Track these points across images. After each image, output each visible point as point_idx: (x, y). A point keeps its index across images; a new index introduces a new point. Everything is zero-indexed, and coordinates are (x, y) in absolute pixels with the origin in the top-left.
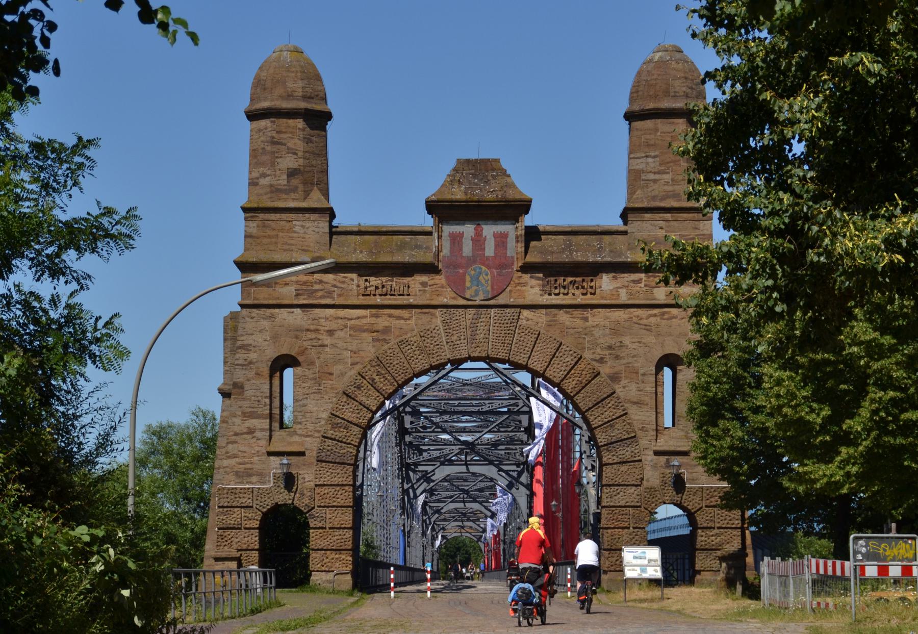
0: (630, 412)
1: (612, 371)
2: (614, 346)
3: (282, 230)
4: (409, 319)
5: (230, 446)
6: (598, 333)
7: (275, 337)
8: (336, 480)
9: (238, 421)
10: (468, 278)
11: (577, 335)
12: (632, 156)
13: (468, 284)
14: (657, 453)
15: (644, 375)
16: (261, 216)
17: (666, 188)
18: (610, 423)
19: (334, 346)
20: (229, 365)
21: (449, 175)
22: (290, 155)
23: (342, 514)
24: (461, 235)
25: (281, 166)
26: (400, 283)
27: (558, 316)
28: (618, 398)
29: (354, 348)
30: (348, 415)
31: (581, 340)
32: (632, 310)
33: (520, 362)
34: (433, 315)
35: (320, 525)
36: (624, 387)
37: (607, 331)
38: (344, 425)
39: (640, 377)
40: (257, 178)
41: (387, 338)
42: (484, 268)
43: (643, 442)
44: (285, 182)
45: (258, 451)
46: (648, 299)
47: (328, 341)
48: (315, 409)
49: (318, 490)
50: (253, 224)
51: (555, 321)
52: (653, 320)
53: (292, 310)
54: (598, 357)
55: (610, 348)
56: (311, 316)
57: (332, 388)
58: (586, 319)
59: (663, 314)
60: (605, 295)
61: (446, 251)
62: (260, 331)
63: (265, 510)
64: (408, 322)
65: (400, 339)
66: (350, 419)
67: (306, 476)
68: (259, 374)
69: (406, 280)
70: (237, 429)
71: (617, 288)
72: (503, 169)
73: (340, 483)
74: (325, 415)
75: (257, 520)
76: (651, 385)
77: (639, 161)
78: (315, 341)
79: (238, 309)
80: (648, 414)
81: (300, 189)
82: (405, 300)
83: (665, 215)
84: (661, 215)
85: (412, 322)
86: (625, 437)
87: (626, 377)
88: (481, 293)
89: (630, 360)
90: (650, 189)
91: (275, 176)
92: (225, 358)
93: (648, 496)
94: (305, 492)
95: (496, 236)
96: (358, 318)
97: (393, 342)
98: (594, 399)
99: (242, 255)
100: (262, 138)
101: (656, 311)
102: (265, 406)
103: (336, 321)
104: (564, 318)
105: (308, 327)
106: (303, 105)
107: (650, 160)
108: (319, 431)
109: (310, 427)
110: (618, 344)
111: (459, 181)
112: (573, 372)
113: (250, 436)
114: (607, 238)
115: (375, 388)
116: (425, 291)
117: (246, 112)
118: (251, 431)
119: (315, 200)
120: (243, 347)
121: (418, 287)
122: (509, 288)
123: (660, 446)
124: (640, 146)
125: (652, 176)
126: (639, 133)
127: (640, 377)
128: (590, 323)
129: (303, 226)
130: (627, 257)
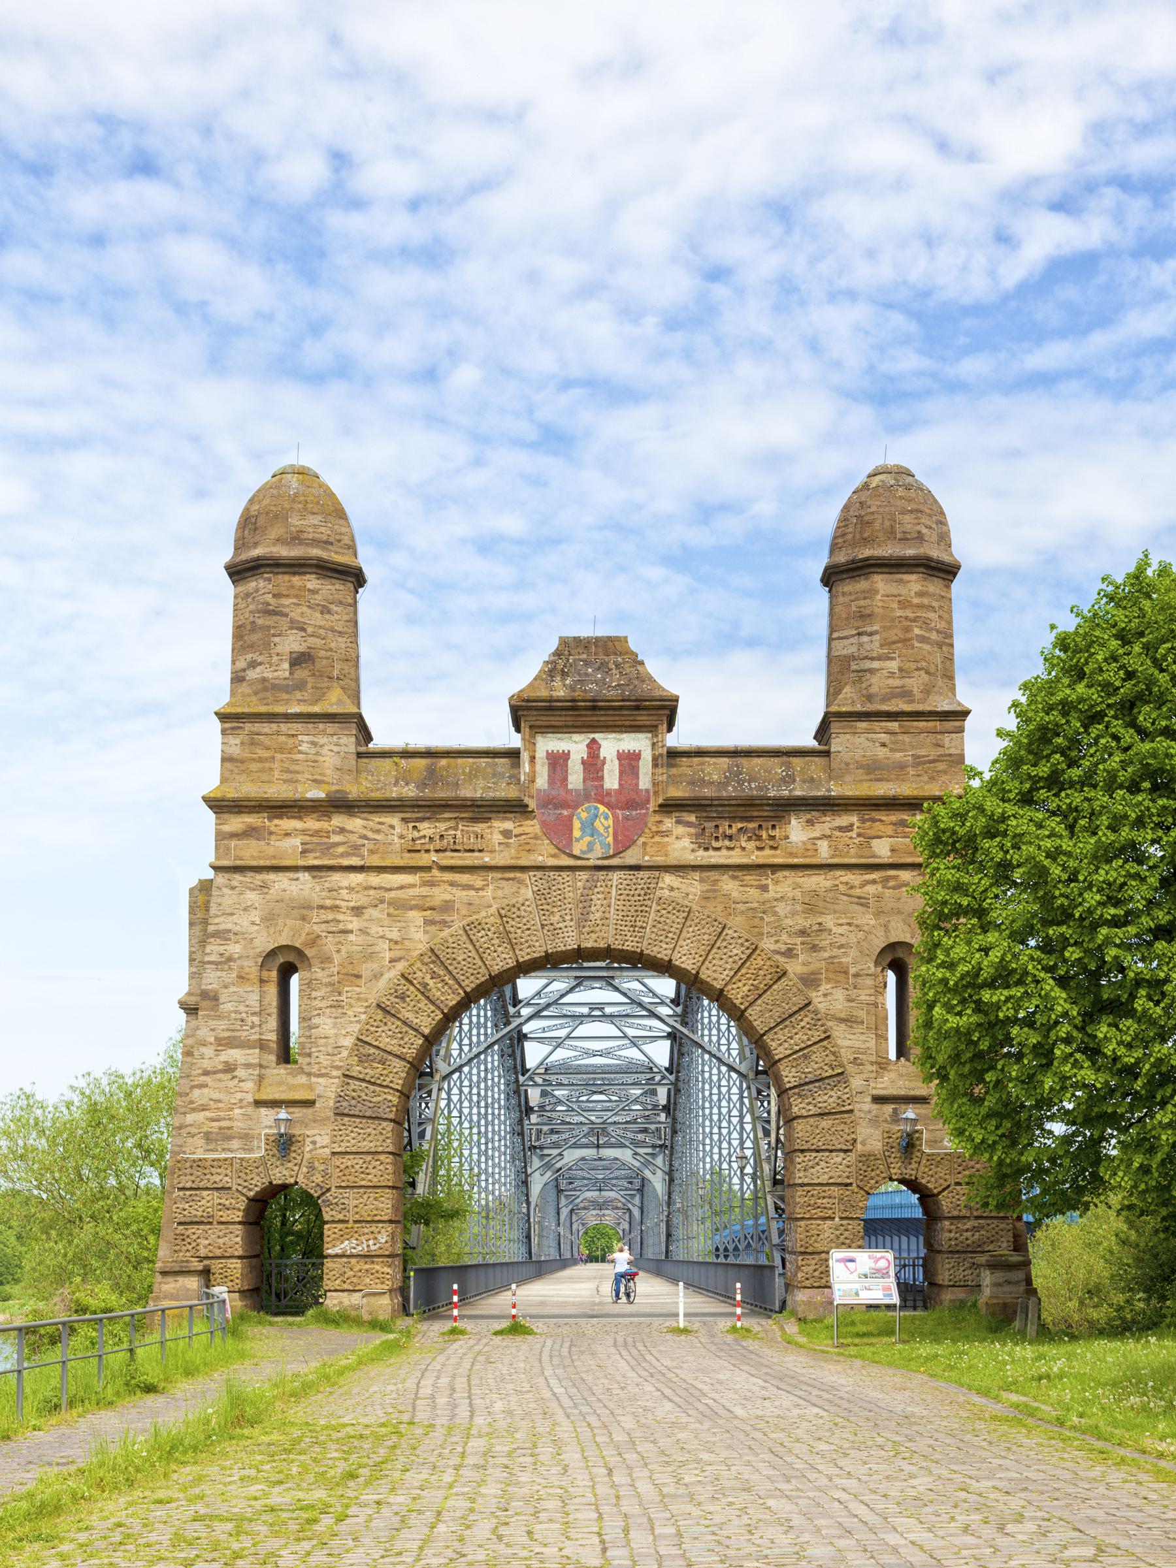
0: (835, 1034)
1: (806, 970)
2: (809, 931)
3: (281, 750)
4: (482, 889)
5: (197, 1092)
6: (782, 909)
7: (269, 919)
8: (366, 1145)
9: (208, 1051)
10: (577, 824)
11: (750, 914)
12: (835, 635)
13: (577, 833)
14: (879, 1100)
15: (856, 975)
16: (248, 727)
17: (891, 682)
18: (802, 1053)
19: (363, 932)
20: (197, 963)
21: (546, 663)
22: (295, 631)
23: (376, 1199)
24: (566, 756)
25: (279, 649)
26: (468, 832)
28: (816, 1012)
29: (395, 935)
30: (385, 1042)
31: (756, 922)
32: (838, 873)
33: (659, 956)
34: (521, 882)
35: (341, 1217)
36: (825, 995)
37: (799, 908)
38: (379, 1058)
40: (244, 670)
41: (448, 919)
42: (602, 808)
43: (857, 1083)
44: (287, 674)
45: (241, 1100)
46: (862, 857)
47: (354, 924)
48: (333, 1031)
49: (337, 1161)
50: (234, 741)
51: (715, 891)
52: (871, 889)
53: (296, 875)
54: (783, 948)
55: (803, 933)
56: (327, 885)
57: (359, 999)
58: (764, 888)
59: (887, 879)
60: (795, 850)
62: (245, 910)
63: (252, 1194)
64: (481, 893)
66: (389, 1048)
67: (317, 1138)
68: (243, 978)
69: (479, 827)
70: (207, 1064)
71: (814, 838)
72: (632, 653)
73: (373, 1150)
74: (348, 1042)
75: (239, 1210)
76: (868, 992)
77: (846, 642)
79: (210, 874)
80: (863, 1038)
82: (477, 858)
83: (889, 724)
84: (883, 724)
85: (489, 893)
86: (827, 1074)
87: (828, 980)
88: (597, 846)
89: (835, 952)
90: (864, 685)
91: (271, 665)
92: (191, 953)
93: (864, 1168)
94: (316, 1164)
95: (621, 756)
96: (402, 888)
97: (458, 925)
98: (777, 1014)
99: (216, 789)
100: (252, 607)
101: (875, 875)
102: (252, 1028)
103: (366, 893)
104: (730, 886)
105: (321, 903)
107: (865, 639)
108: (338, 1068)
109: (325, 1060)
110: (816, 927)
111: (562, 670)
112: (743, 971)
113: (229, 1076)
114: (797, 762)
115: (428, 998)
116: (508, 845)
117: (227, 568)
118: (229, 1068)
119: (334, 701)
120: (217, 934)
121: (497, 837)
122: (642, 840)
124: (847, 619)
126: (847, 599)
128: (771, 894)
129: (314, 743)
130: (829, 790)
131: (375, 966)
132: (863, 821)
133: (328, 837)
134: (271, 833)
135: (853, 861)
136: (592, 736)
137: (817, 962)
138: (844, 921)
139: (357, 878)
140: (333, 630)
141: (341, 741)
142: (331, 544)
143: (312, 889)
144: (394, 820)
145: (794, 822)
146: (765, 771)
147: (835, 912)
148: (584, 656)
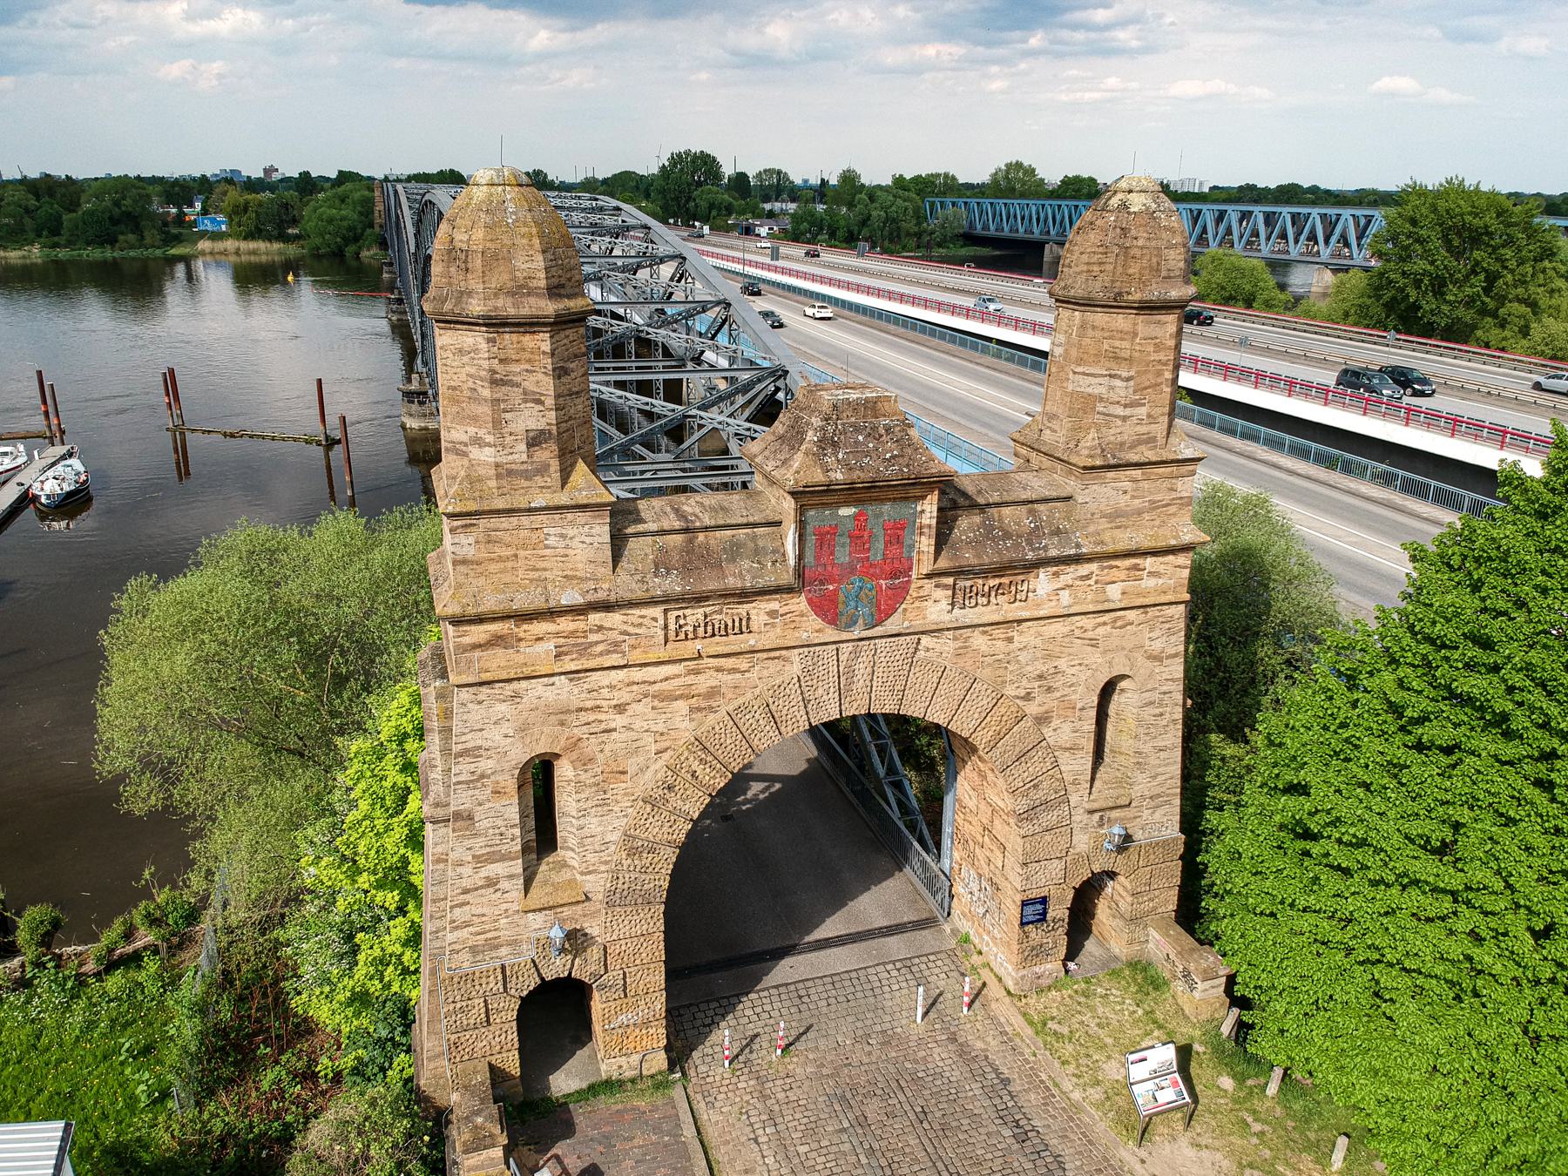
0: (1060, 761)
3: (524, 547)
5: (457, 911)
6: (1023, 657)
7: (523, 729)
9: (467, 870)
10: (841, 598)
14: (1091, 812)
16: (483, 523)
19: (628, 728)
22: (528, 405)
24: (833, 531)
25: (512, 427)
29: (660, 727)
34: (786, 660)
39: (1078, 713)
41: (714, 704)
44: (524, 457)
45: (506, 910)
47: (619, 721)
51: (966, 647)
52: (1101, 630)
54: (1022, 693)
55: (1041, 677)
56: (586, 686)
57: (625, 794)
58: (1010, 640)
62: (495, 723)
65: (736, 704)
70: (467, 883)
74: (615, 837)
80: (1083, 761)
81: (552, 469)
84: (1128, 473)
87: (1059, 716)
96: (666, 679)
101: (1107, 617)
102: (512, 840)
103: (628, 689)
106: (549, 308)
107: (1118, 383)
108: (606, 863)
109: (591, 857)
110: (1051, 671)
112: (988, 719)
113: (492, 890)
116: (773, 625)
118: (491, 883)
122: (903, 606)
123: (1093, 801)
125: (1120, 411)
127: (1078, 713)
128: (1016, 645)
129: (563, 536)
131: (641, 759)
134: (520, 640)
135: (1091, 608)
137: (1050, 702)
139: (622, 674)
142: (563, 286)
144: (657, 611)
145: (1042, 575)
148: (853, 419)
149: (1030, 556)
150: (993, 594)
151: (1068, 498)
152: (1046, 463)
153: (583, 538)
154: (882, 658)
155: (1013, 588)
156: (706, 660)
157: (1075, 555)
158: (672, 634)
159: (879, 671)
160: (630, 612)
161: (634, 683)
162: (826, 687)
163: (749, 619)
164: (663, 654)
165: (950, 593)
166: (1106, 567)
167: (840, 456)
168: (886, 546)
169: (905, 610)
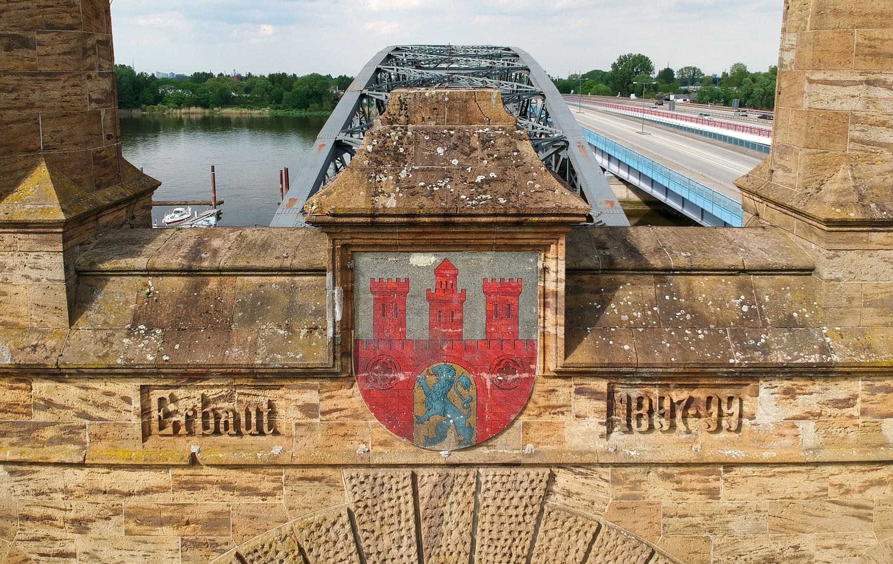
6: (737, 524)
10: (419, 394)
13: (419, 410)
24: (402, 287)
27: (644, 486)
31: (698, 545)
34: (333, 484)
41: (220, 540)
51: (635, 497)
56: (32, 485)
58: (713, 494)
61: (365, 327)
64: (270, 500)
78: (44, 543)
85: (281, 501)
96: (146, 491)
103: (92, 499)
110: (790, 552)
116: (310, 427)
122: (523, 419)
128: (723, 503)
132: (873, 391)
133: (29, 414)
135: (855, 455)
136: (444, 256)
138: (833, 542)
139: (81, 476)
140: (34, 74)
141: (41, 262)
143: (11, 490)
144: (130, 388)
145: (764, 393)
146: (716, 303)
147: (821, 528)
148: (432, 124)
149: (737, 358)
150: (679, 414)
151: (808, 271)
152: (779, 217)
153: (27, 271)
154: (487, 498)
155: (714, 409)
156: (207, 471)
157: (819, 365)
158: (155, 425)
159: (484, 522)
160: (90, 384)
161: (99, 491)
162: (396, 535)
163: (272, 412)
164: (136, 451)
165: (603, 405)
166: (880, 389)
167: (403, 174)
168: (489, 319)
169: (526, 425)
